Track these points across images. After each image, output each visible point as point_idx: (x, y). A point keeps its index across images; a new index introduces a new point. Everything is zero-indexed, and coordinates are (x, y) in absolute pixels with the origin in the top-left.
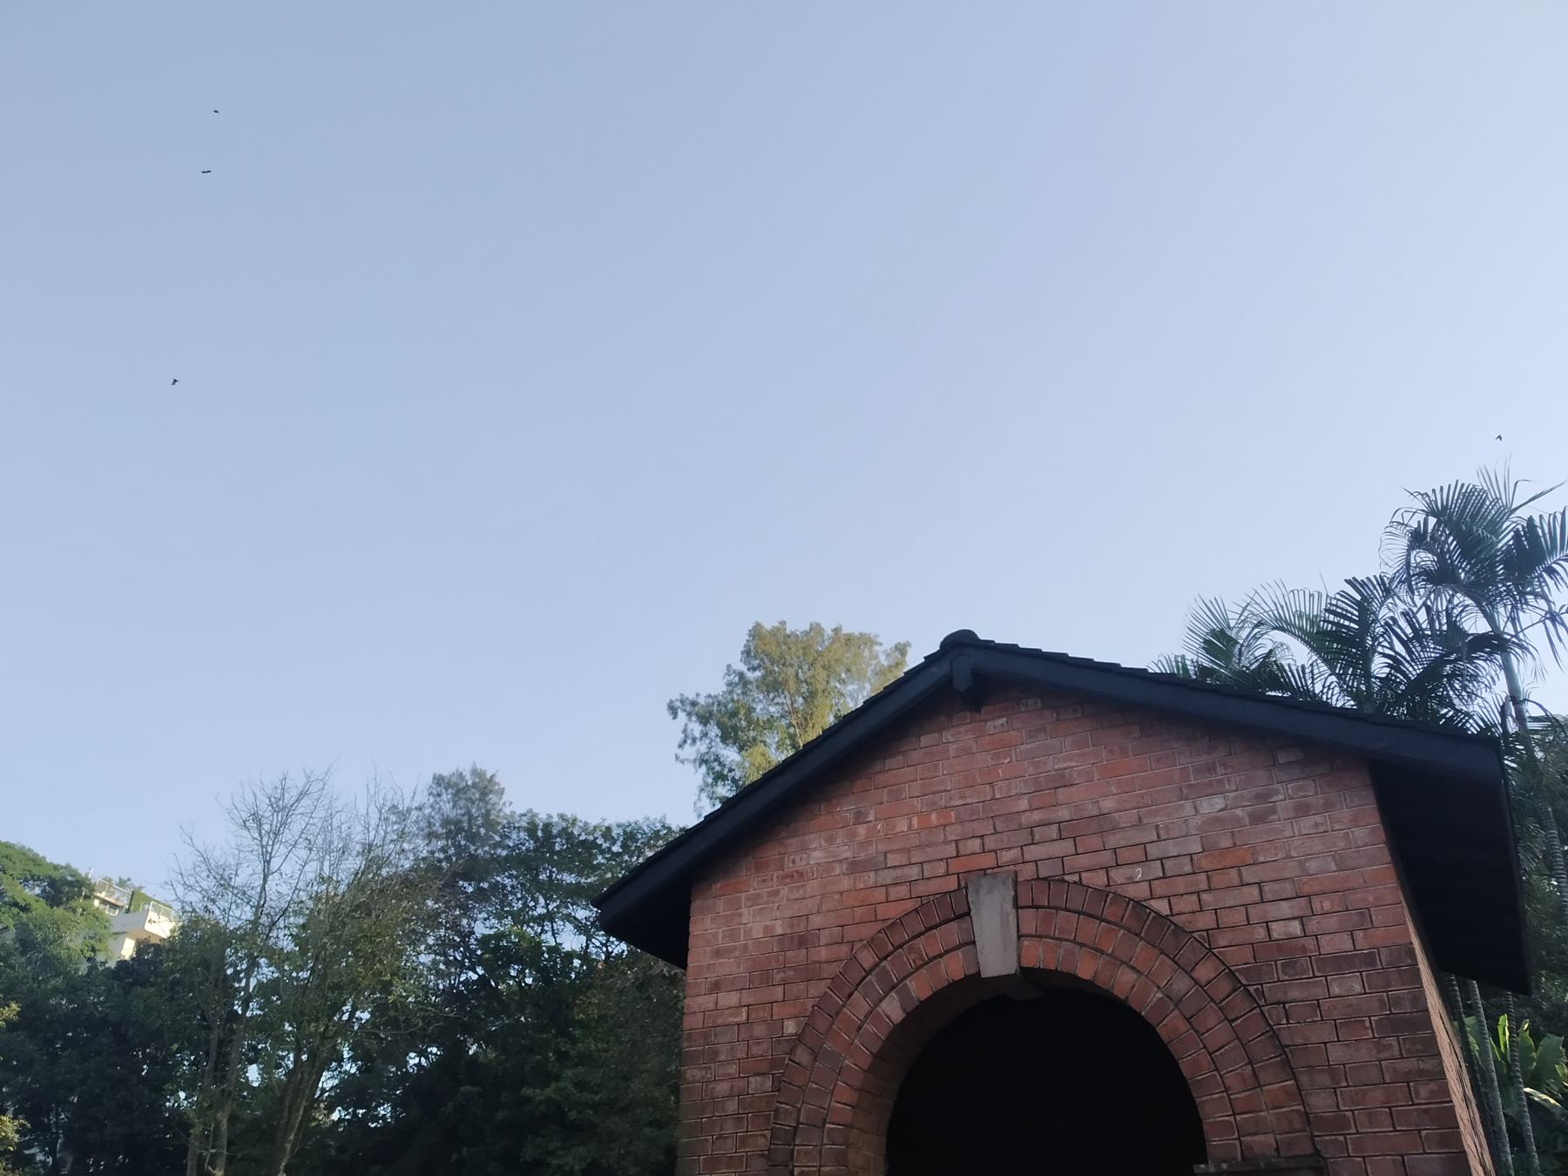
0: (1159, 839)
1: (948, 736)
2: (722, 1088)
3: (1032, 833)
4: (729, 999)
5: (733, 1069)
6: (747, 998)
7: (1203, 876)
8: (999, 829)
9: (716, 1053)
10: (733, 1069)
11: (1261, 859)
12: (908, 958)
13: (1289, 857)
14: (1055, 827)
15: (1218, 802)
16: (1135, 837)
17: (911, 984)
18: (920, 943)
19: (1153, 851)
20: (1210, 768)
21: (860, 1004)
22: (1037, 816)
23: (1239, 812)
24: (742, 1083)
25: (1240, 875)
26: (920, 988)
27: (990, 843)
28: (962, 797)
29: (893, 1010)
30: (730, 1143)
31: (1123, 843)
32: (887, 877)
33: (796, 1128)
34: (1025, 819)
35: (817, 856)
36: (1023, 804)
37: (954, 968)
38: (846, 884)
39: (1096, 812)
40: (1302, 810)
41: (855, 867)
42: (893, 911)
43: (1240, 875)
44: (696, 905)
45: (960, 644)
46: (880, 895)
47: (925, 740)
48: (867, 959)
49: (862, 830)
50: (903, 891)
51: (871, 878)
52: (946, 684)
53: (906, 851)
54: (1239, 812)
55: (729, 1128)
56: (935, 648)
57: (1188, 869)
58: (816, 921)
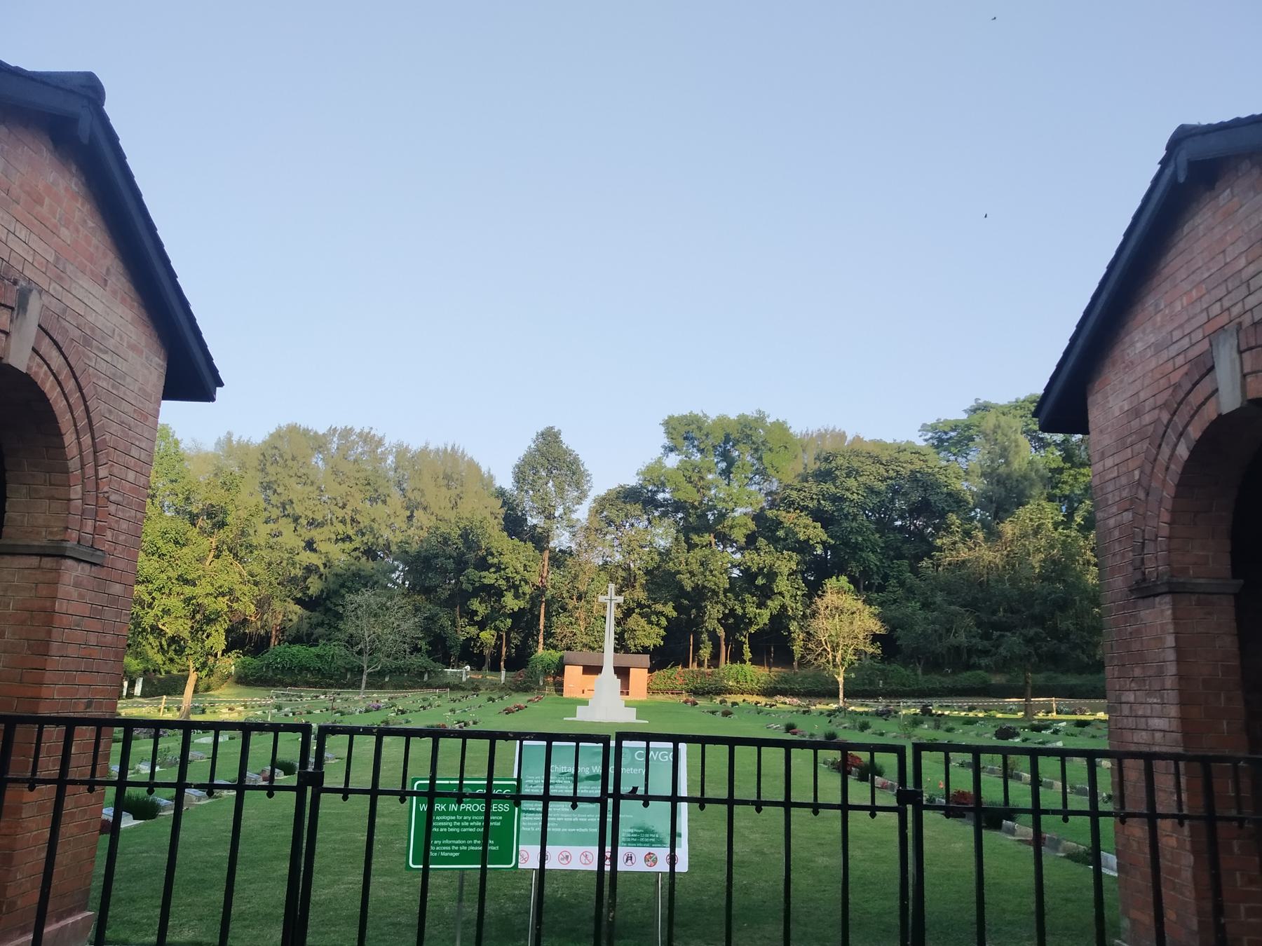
2: (1112, 522)
3: (1248, 286)
4: (1109, 462)
5: (1114, 509)
6: (1117, 459)
9: (1107, 499)
10: (1114, 509)
12: (1185, 411)
18: (1191, 397)
21: (1166, 451)
24: (1119, 518)
26: (1195, 432)
27: (1226, 303)
28: (1209, 270)
29: (1183, 451)
30: (1118, 558)
32: (1174, 350)
33: (1143, 543)
34: (1245, 275)
35: (1139, 346)
36: (1242, 262)
37: (1210, 413)
41: (1158, 348)
42: (1175, 378)
44: (1090, 400)
45: (1182, 138)
46: (1170, 366)
48: (1165, 417)
49: (1159, 318)
50: (1180, 360)
51: (1164, 355)
53: (1181, 326)
55: (1117, 547)
56: (1163, 153)
58: (1142, 396)
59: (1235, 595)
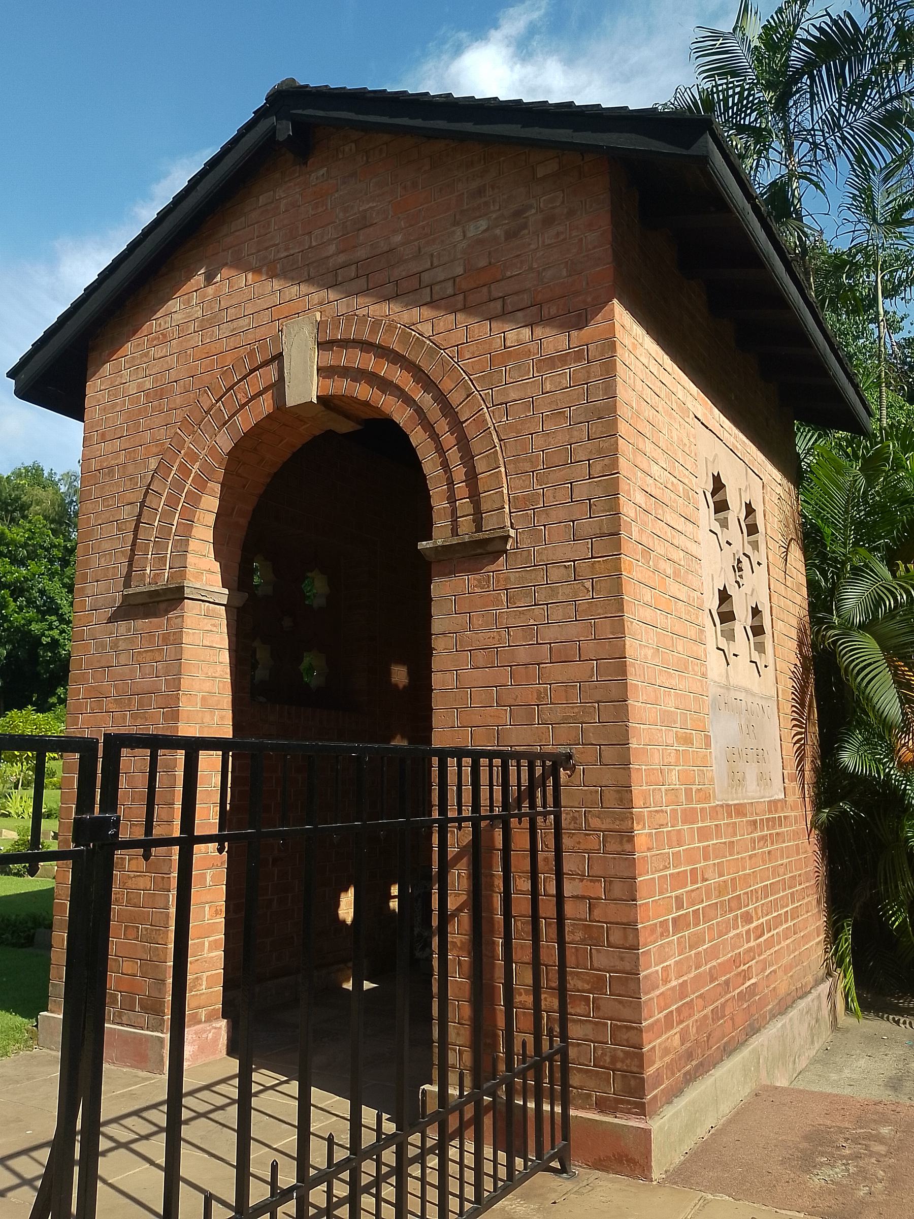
0: (433, 267)
1: (280, 193)
7: (461, 297)
8: (312, 275)
11: (509, 274)
13: (531, 268)
14: (354, 267)
15: (483, 224)
16: (414, 267)
17: (238, 419)
19: (426, 277)
20: (480, 192)
22: (341, 259)
23: (498, 231)
25: (490, 292)
28: (287, 249)
29: (225, 442)
31: (404, 274)
36: (332, 249)
38: (197, 339)
39: (385, 249)
40: (549, 221)
43: (490, 292)
47: (262, 200)
52: (270, 139)
54: (498, 231)
57: (450, 291)
59: (238, 608)
